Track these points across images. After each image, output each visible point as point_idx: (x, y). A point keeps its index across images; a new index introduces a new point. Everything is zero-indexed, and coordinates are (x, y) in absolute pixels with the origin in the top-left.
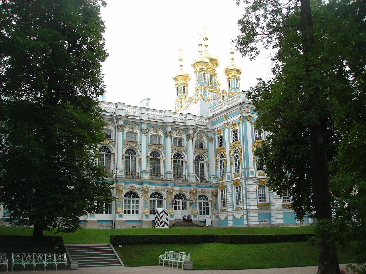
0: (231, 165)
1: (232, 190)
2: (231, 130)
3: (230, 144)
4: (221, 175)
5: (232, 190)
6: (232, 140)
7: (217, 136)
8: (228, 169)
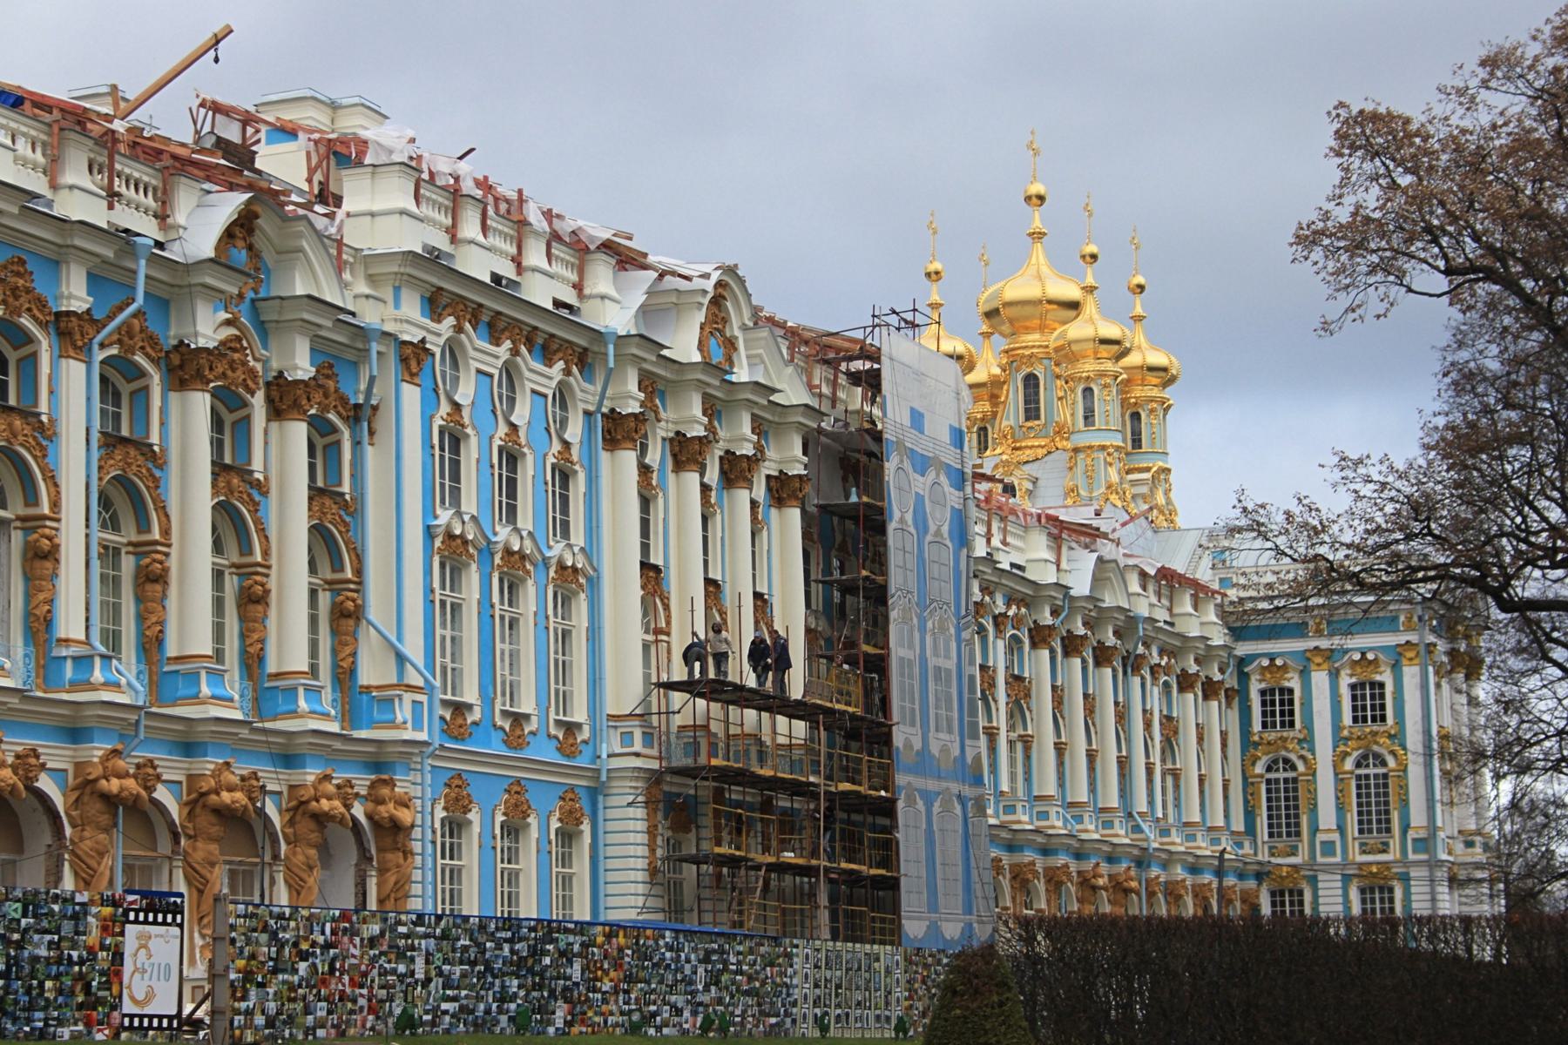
0: (1341, 808)
1: (1346, 895)
2: (1345, 681)
3: (1337, 726)
4: (1271, 835)
5: (1346, 895)
6: (1347, 719)
7: (1255, 687)
8: (1327, 815)
